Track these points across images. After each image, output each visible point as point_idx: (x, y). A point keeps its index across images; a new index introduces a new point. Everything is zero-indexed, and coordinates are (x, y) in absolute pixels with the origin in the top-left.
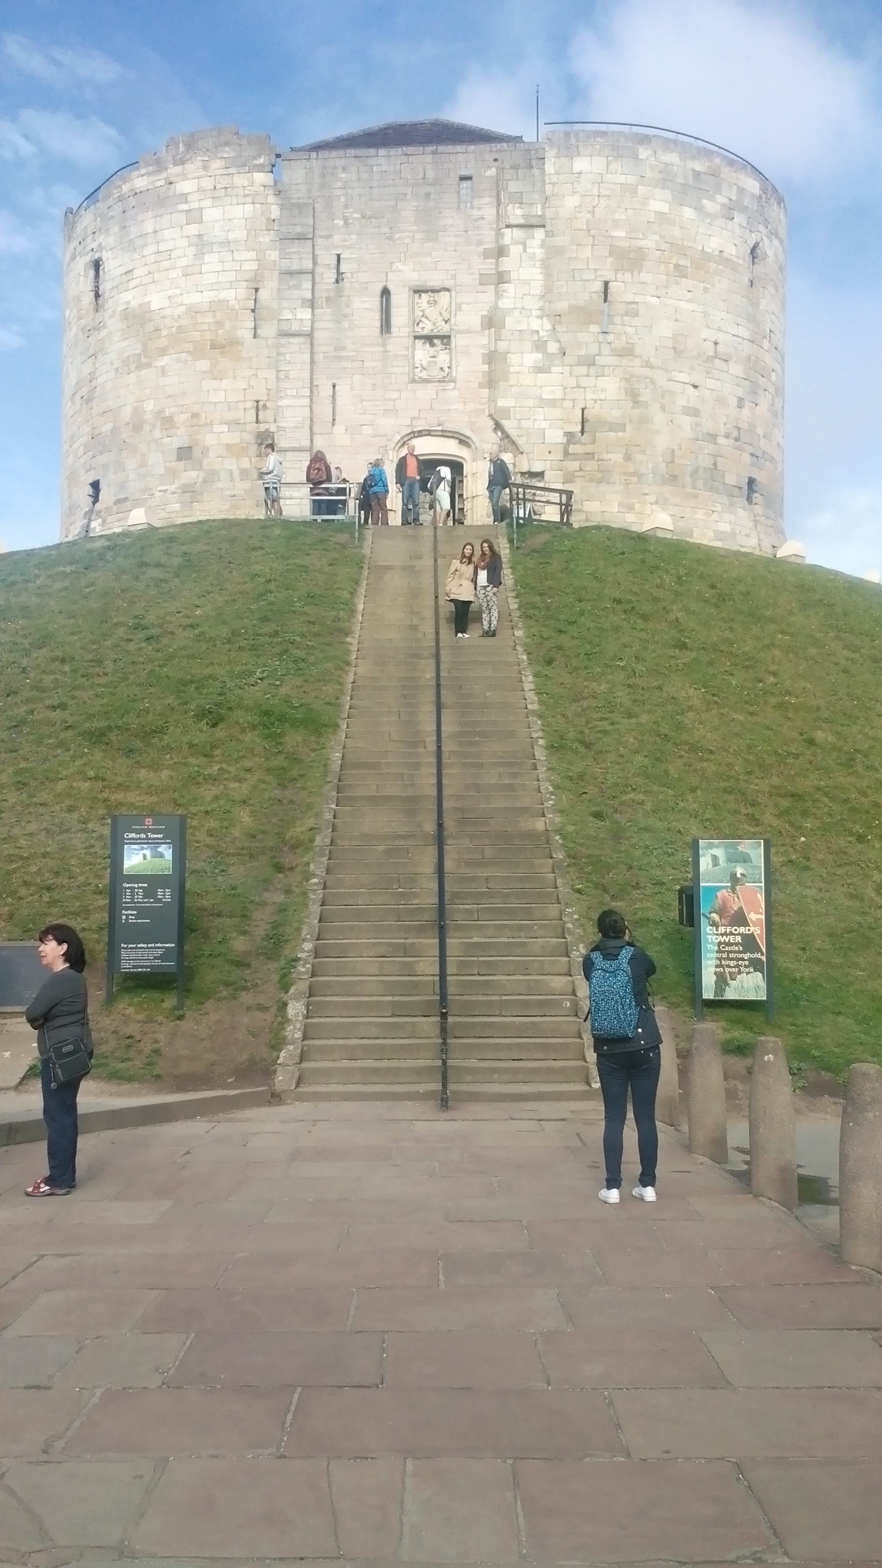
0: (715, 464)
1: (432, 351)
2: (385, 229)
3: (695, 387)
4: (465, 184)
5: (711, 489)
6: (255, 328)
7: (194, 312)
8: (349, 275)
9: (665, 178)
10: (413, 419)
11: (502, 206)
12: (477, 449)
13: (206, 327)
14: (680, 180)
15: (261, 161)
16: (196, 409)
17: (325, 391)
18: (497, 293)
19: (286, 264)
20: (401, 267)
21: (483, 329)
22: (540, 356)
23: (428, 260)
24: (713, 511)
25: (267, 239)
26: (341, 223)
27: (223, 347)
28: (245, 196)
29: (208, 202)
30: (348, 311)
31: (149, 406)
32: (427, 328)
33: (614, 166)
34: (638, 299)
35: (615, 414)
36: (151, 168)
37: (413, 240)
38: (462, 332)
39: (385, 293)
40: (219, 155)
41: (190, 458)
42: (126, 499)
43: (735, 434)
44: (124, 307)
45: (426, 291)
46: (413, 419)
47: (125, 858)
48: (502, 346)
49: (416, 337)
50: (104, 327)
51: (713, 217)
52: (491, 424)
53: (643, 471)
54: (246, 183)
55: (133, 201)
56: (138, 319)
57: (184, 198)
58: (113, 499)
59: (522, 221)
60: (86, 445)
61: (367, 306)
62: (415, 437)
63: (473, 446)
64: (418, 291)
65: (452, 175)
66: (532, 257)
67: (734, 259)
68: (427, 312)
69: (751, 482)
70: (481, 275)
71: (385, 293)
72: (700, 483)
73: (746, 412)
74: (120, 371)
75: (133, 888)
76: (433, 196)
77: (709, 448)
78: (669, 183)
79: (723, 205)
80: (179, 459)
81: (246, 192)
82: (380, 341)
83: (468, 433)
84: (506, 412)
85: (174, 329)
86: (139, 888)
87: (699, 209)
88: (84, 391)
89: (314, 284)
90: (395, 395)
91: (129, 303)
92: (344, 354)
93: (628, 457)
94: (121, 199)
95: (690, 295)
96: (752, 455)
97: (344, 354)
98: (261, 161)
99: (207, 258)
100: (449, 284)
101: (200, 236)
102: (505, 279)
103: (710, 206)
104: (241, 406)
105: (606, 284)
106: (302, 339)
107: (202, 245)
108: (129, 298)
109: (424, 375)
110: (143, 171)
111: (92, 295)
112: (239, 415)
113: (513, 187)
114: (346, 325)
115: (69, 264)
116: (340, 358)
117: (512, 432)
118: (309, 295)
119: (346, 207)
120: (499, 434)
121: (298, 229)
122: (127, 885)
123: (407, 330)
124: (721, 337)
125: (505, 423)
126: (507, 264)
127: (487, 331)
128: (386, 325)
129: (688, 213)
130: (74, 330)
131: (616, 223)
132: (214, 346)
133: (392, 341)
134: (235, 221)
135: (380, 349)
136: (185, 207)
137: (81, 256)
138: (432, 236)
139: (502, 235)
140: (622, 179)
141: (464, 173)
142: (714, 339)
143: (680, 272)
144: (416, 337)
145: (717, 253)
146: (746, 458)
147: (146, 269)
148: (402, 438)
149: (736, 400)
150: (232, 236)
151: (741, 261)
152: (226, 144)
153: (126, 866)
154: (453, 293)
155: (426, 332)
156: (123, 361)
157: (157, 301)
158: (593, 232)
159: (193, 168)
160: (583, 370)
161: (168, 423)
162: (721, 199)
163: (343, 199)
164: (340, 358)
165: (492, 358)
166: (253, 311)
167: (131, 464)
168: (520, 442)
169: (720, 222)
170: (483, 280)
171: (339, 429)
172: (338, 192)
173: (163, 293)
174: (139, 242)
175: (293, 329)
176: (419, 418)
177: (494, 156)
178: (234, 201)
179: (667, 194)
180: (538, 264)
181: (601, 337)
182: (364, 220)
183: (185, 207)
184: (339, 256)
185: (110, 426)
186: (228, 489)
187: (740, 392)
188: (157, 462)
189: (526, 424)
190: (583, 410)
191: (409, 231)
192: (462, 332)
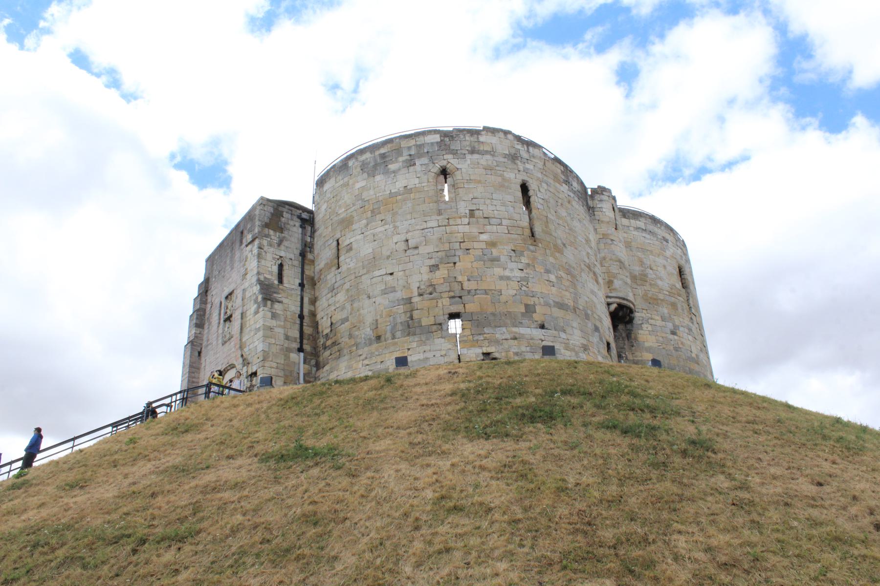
0: (411, 318)
5: (408, 335)
14: (372, 164)
24: (409, 349)
34: (352, 240)
43: (431, 289)
53: (359, 341)
72: (398, 334)
73: (442, 273)
79: (403, 161)
87: (387, 172)
93: (351, 336)
103: (392, 167)
105: (338, 241)
124: (409, 236)
131: (340, 207)
140: (341, 182)
142: (404, 239)
146: (446, 301)
160: (330, 295)
165: (243, 315)
169: (404, 171)
179: (365, 175)
187: (432, 262)
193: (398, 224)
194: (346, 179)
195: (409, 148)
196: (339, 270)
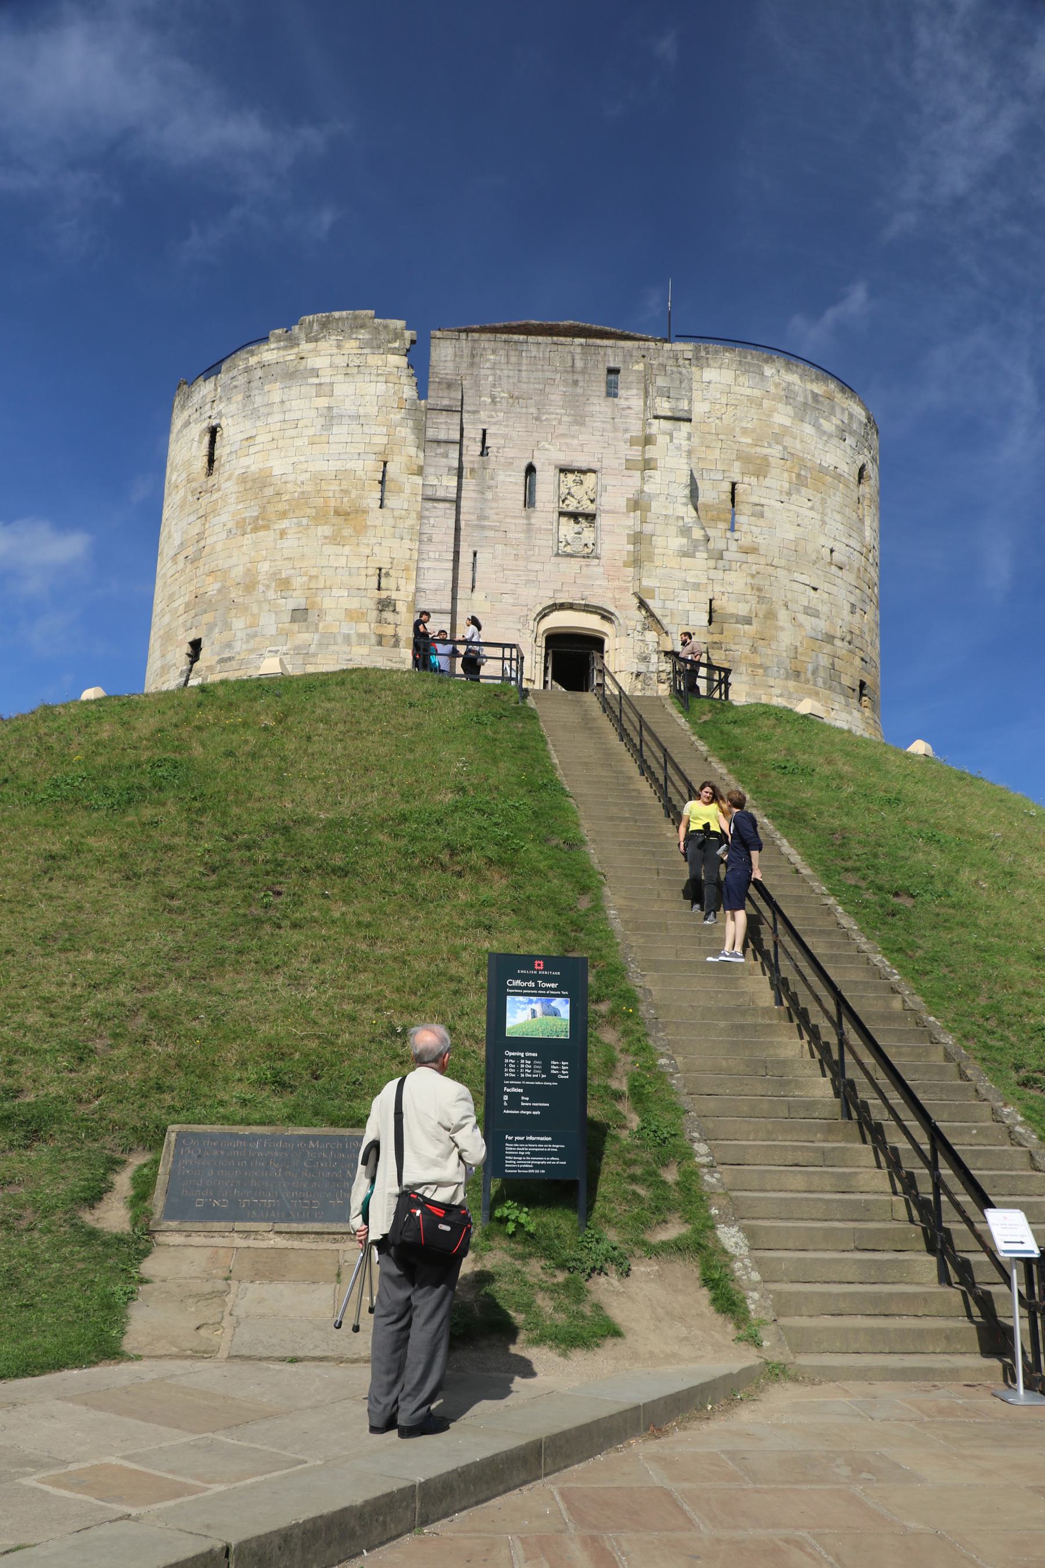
0: (833, 664)
1: (577, 528)
2: (533, 410)
3: (815, 589)
4: (612, 377)
5: (830, 688)
6: (382, 500)
7: (318, 479)
8: (495, 450)
9: (789, 396)
10: (555, 591)
11: (650, 398)
12: (620, 625)
13: (331, 494)
14: (800, 399)
15: (396, 345)
16: (314, 572)
17: (466, 558)
18: (643, 478)
19: (431, 433)
20: (547, 446)
21: (628, 511)
22: (685, 541)
23: (575, 442)
25: (399, 417)
26: (489, 400)
27: (348, 515)
28: (378, 375)
29: (340, 378)
30: (492, 483)
31: (265, 567)
32: (572, 506)
33: (741, 379)
34: (763, 501)
35: (742, 609)
36: (282, 343)
37: (560, 423)
38: (608, 512)
39: (530, 470)
40: (354, 336)
41: (305, 620)
42: (230, 659)
43: (848, 638)
44: (243, 471)
45: (572, 471)
46: (555, 591)
47: (508, 1014)
48: (648, 528)
49: (561, 514)
50: (219, 490)
51: (830, 436)
52: (636, 601)
53: (768, 664)
54: (380, 363)
55: (259, 373)
56: (256, 484)
57: (315, 372)
58: (217, 658)
59: (670, 414)
60: (187, 605)
61: (512, 479)
62: (556, 609)
63: (616, 622)
64: (563, 470)
65: (601, 366)
66: (679, 448)
67: (846, 475)
68: (572, 491)
69: (862, 685)
70: (627, 460)
71: (530, 470)
74: (233, 531)
75: (518, 1058)
76: (581, 384)
77: (828, 648)
78: (791, 401)
79: (837, 426)
80: (293, 620)
81: (379, 372)
82: (524, 514)
83: (612, 609)
84: (651, 592)
85: (296, 494)
86: (525, 1058)
87: (817, 426)
88: (190, 551)
89: (461, 454)
90: (538, 567)
91: (248, 467)
92: (486, 523)
93: (754, 649)
94: (247, 370)
95: (810, 504)
96: (862, 659)
97: (486, 523)
98: (396, 345)
99: (335, 429)
100: (593, 466)
101: (330, 408)
102: (652, 465)
104: (363, 572)
105: (734, 485)
106: (447, 505)
107: (330, 417)
108: (251, 463)
109: (568, 549)
110: (272, 346)
111: (205, 459)
112: (361, 581)
113: (661, 382)
114: (489, 495)
115: (180, 431)
116: (483, 527)
117: (657, 612)
118: (456, 464)
119: (494, 386)
120: (644, 612)
121: (446, 402)
122: (510, 1054)
123: (553, 505)
124: (837, 546)
125: (650, 602)
126: (652, 452)
127: (632, 514)
128: (529, 501)
129: (808, 429)
130: (182, 492)
132: (337, 513)
133: (536, 514)
134: (368, 398)
135: (525, 522)
136: (316, 381)
137: (196, 421)
138: (580, 420)
139: (650, 424)
140: (749, 391)
141: (612, 365)
143: (800, 481)
144: (561, 514)
145: (832, 468)
147: (270, 435)
148: (544, 609)
149: (849, 605)
150: (362, 411)
151: (851, 479)
152: (362, 327)
153: (508, 1025)
154: (599, 475)
155: (571, 509)
156: (238, 523)
157: (279, 466)
158: (720, 437)
159: (327, 345)
161: (285, 585)
162: (835, 421)
163: (491, 378)
164: (483, 527)
165: (637, 538)
166: (382, 482)
167: (238, 624)
168: (665, 621)
169: (835, 441)
170: (630, 465)
171: (479, 595)
172: (489, 372)
173: (287, 459)
174: (262, 410)
175: (438, 494)
176: (561, 591)
177: (643, 353)
178: (367, 378)
179: (790, 410)
180: (684, 454)
181: (729, 534)
182: (511, 400)
183: (316, 381)
184: (484, 431)
185: (217, 586)
186: (345, 653)
188: (269, 623)
189: (669, 604)
190: (711, 601)
191: (557, 414)
192: (608, 512)
193: (826, 519)
194: (757, 393)
195: (843, 410)
196: (737, 535)
